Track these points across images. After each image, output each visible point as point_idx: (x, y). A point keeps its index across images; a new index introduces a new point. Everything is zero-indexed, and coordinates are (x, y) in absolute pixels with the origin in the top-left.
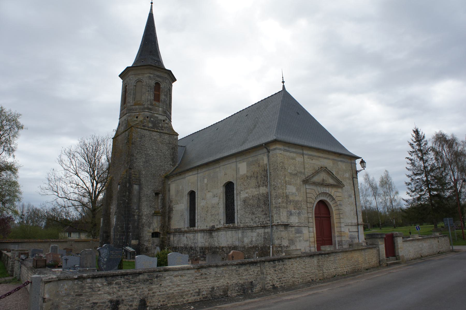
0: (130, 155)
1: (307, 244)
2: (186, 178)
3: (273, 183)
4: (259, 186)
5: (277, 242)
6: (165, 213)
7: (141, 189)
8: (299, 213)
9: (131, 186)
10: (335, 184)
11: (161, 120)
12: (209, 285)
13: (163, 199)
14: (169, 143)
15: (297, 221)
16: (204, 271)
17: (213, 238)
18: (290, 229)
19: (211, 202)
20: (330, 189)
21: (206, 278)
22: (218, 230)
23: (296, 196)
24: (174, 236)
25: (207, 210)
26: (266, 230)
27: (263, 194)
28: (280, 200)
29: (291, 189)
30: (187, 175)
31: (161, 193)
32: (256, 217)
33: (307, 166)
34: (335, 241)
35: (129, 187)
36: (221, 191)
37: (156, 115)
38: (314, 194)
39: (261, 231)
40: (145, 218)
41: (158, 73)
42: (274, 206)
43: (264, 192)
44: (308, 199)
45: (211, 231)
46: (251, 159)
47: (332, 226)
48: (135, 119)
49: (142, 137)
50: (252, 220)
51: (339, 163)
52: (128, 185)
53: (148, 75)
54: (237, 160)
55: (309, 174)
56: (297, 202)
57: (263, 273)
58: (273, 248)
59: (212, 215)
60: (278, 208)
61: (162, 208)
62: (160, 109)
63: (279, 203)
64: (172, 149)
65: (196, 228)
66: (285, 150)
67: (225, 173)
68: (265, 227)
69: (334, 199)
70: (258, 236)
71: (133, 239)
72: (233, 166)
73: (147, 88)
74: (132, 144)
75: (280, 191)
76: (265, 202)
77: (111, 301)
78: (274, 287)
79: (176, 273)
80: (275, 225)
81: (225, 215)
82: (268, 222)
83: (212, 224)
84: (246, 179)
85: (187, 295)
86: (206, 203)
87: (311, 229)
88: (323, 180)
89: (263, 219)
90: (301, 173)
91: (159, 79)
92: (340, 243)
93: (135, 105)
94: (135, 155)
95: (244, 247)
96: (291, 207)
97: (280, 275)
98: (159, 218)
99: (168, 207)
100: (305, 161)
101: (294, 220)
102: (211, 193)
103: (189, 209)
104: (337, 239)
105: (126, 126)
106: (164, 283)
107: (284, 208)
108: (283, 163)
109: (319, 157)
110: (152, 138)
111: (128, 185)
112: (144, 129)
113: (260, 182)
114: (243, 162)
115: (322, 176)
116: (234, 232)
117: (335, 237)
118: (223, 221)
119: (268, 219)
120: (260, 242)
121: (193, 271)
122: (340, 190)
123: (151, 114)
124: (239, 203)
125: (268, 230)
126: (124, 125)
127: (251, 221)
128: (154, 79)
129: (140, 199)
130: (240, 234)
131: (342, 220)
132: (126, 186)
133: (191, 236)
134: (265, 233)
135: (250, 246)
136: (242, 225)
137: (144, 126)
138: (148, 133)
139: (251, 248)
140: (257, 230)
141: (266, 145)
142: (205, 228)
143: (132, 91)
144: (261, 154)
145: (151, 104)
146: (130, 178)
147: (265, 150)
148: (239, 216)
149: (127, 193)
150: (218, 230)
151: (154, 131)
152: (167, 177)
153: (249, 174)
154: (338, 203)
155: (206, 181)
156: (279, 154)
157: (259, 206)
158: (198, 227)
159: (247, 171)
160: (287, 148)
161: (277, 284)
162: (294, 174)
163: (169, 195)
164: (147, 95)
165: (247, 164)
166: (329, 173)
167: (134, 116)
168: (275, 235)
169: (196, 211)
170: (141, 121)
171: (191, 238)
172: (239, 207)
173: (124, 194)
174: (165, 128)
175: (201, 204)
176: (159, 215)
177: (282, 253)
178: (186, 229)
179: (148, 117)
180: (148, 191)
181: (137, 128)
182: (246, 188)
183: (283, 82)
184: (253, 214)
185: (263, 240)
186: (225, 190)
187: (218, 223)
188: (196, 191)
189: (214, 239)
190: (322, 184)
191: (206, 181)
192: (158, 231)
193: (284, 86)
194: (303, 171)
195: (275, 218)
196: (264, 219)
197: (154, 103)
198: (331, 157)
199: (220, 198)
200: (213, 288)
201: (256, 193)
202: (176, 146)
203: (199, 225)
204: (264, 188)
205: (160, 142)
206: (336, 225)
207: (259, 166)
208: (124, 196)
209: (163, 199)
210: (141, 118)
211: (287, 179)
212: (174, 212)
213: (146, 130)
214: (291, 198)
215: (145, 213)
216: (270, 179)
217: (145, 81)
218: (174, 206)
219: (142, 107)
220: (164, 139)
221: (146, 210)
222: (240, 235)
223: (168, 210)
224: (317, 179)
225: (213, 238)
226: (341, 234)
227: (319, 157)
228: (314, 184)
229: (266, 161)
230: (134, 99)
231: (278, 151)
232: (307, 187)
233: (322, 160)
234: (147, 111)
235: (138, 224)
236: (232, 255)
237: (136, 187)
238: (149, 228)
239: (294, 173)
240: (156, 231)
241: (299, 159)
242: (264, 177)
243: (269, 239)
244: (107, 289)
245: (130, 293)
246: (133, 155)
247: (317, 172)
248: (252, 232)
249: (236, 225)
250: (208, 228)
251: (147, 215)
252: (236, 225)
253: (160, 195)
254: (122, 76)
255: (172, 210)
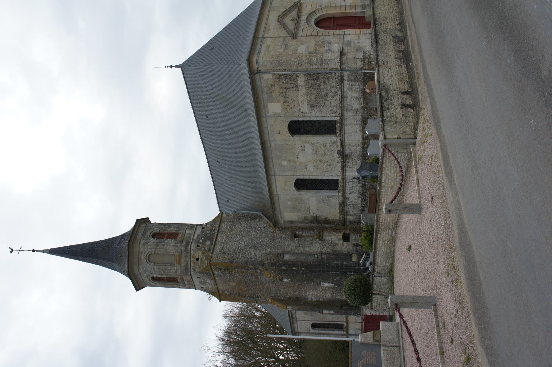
0: (245, 266)
1: (362, 36)
2: (279, 193)
3: (295, 67)
4: (297, 86)
5: (359, 64)
6: (319, 226)
7: (289, 252)
8: (329, 43)
9: (285, 263)
10: (297, 9)
11: (202, 231)
12: (393, 60)
13: (302, 229)
14: (233, 222)
15: (337, 45)
16: (381, 63)
17: (352, 153)
18: (346, 50)
19: (311, 156)
20: (303, 14)
21: (387, 62)
22: (342, 144)
23: (309, 45)
24: (349, 215)
25: (318, 162)
26: (346, 78)
27: (305, 81)
28: (314, 59)
29: (302, 49)
30: (275, 193)
31: (295, 231)
32: (331, 92)
33: (277, 35)
34: (361, 12)
35: (286, 267)
36: (298, 140)
37: (195, 237)
38: (307, 29)
39: (346, 84)
40: (325, 249)
41: (140, 235)
42: (319, 66)
43: (304, 79)
44: (313, 34)
45: (344, 155)
46: (265, 96)
47: (344, 15)
48: (199, 261)
49: (223, 252)
50: (333, 97)
51: (273, 5)
52: (284, 268)
53: (141, 246)
54: (264, 115)
55: (286, 33)
56: (316, 45)
57: (386, 31)
58: (365, 70)
59: (326, 155)
60: (322, 61)
61: (313, 230)
62: (187, 232)
63: (317, 59)
64: (239, 219)
65: (340, 178)
66: (259, 52)
67: (278, 132)
68: (342, 80)
69: (314, 12)
70: (351, 89)
71: (351, 260)
72: (270, 121)
73: (159, 247)
74: (232, 262)
75: (304, 58)
76: (315, 77)
77: (402, 108)
78: (400, 24)
79: (381, 77)
80: (341, 65)
81: (326, 136)
82: (337, 74)
83: (336, 155)
84: (287, 104)
85: (400, 72)
86: (310, 162)
87: (346, 33)
88: (292, 20)
89: (333, 83)
90: (284, 41)
91: (148, 234)
92: (364, 7)
93: (180, 263)
94: (246, 260)
95: (363, 108)
96: (322, 50)
97: (389, 21)
98: (326, 234)
99: (312, 225)
100: (271, 36)
101: (336, 47)
102: (300, 155)
103: (317, 191)
104: (359, 10)
105: (207, 274)
106: (390, 82)
107: (322, 55)
108: (273, 56)
109: (266, 23)
110: (225, 241)
111: (284, 268)
112: (213, 250)
113: (292, 85)
114: (267, 107)
115: (288, 21)
116: (346, 122)
117: (356, 13)
118: (333, 138)
119: (333, 75)
120: (358, 86)
121: (381, 69)
122: (304, 6)
123: (194, 242)
124: (313, 114)
125: (346, 74)
126: (206, 278)
127: (335, 98)
128: (148, 238)
129: (301, 254)
130: (348, 114)
131: (339, 4)
132: (285, 270)
133: (348, 186)
134: (348, 80)
135: (362, 100)
136: (339, 111)
137: (209, 250)
138: (219, 245)
139: (364, 99)
140: (346, 90)
141: (253, 73)
142: (340, 165)
143: (162, 267)
144: (261, 83)
145: (181, 242)
146: (275, 265)
147: (257, 76)
148: (328, 115)
149: (294, 268)
150: (342, 144)
151: (216, 239)
152: (275, 224)
153: (282, 100)
154: (318, 7)
155: (284, 163)
156: (263, 59)
157: (319, 87)
158: (338, 176)
159: (278, 102)
160: (257, 52)
161: (398, 22)
162: (286, 46)
163: (298, 222)
164: (168, 247)
165: (270, 102)
166: (285, 14)
167: (195, 263)
168: (352, 66)
169: (320, 178)
170: (203, 253)
171: (351, 186)
172: (318, 114)
173: (295, 272)
174: (212, 227)
175: (312, 170)
176: (321, 234)
177: (371, 57)
178: (340, 194)
179: (198, 246)
180: (292, 245)
181: (211, 257)
182: (298, 103)
183: (171, 67)
184: (326, 95)
185: (356, 83)
186: (297, 135)
187: (335, 145)
188: (296, 178)
189: (353, 151)
190: (297, 21)
191: (284, 163)
192: (342, 235)
193: (176, 66)
194: (282, 39)
195: (333, 66)
196: (333, 80)
197: (179, 239)
198: (266, 12)
199: (306, 142)
200: (396, 58)
201: (304, 90)
202: (236, 215)
203: (335, 174)
204: (299, 79)
205: (230, 232)
206: (343, 11)
207: (274, 85)
208: (298, 273)
209: (302, 229)
210: (199, 254)
211: (291, 53)
212: (319, 214)
213: (214, 247)
214: (312, 50)
215: (319, 248)
216: (289, 70)
217: (149, 251)
218: (312, 214)
219: (183, 254)
220: (226, 228)
221: (316, 248)
222: (350, 114)
223: (316, 225)
224: (291, 25)
225: (352, 153)
226: (353, 6)
227: (266, 23)
228: (297, 27)
229: (268, 76)
230: (172, 264)
231: (260, 60)
232: (300, 35)
233: (269, 21)
234: (189, 247)
235: (333, 254)
236: (370, 89)
237: (287, 257)
238: (337, 244)
239: (284, 46)
240: (341, 237)
241: (268, 41)
242: (286, 78)
243: (355, 73)
244: (392, 110)
245: (396, 99)
246: (247, 262)
247: (284, 26)
248: (347, 97)
249: (338, 119)
250: (340, 160)
251: (321, 247)
252: (338, 119)
253: (297, 233)
254: (138, 287)
255: (316, 217)
